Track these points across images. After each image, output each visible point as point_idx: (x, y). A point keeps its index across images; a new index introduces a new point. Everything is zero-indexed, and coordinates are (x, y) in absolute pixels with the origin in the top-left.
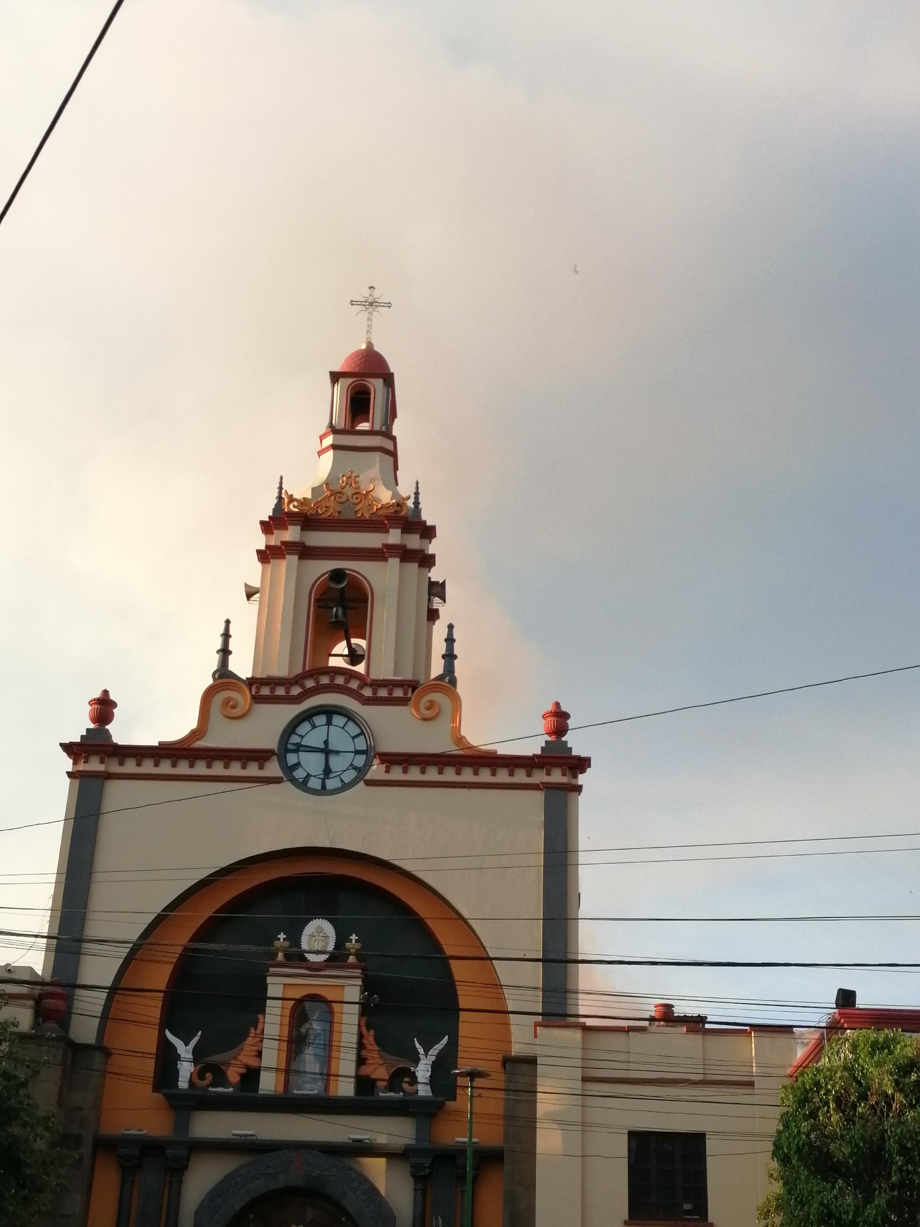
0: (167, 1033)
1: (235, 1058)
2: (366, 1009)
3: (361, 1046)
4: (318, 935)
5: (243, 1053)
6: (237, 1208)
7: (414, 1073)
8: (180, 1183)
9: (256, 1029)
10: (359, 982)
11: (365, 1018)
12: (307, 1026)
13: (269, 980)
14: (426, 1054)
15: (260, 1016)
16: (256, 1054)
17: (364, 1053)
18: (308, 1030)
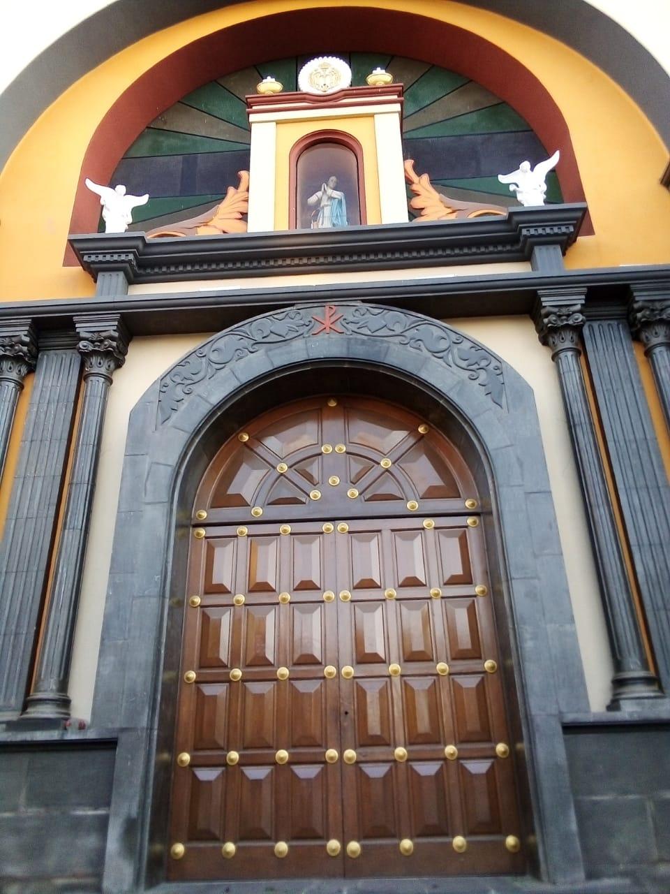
0: (90, 184)
1: (207, 225)
2: (411, 148)
3: (411, 194)
4: (325, 73)
5: (216, 219)
6: (216, 397)
7: (515, 192)
8: (109, 380)
9: (237, 187)
10: (397, 107)
11: (410, 162)
12: (319, 194)
13: (252, 118)
14: (532, 169)
15: (243, 173)
16: (240, 216)
17: (417, 203)
18: (319, 201)
